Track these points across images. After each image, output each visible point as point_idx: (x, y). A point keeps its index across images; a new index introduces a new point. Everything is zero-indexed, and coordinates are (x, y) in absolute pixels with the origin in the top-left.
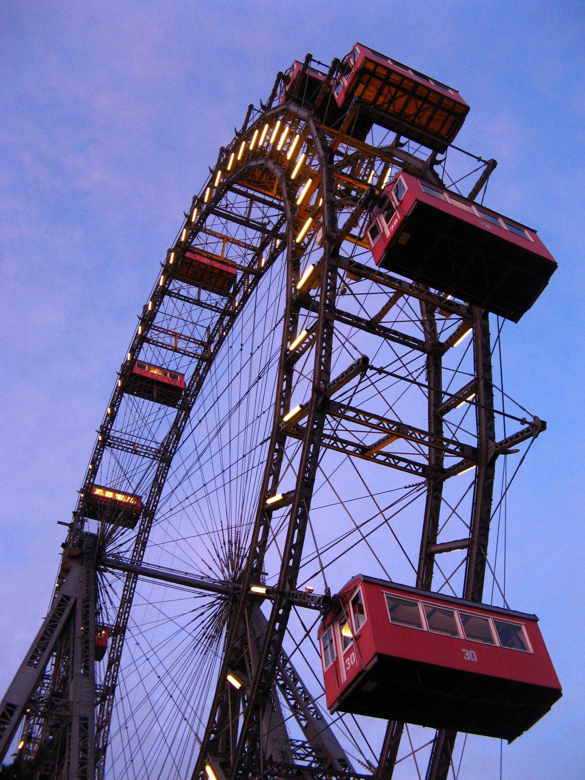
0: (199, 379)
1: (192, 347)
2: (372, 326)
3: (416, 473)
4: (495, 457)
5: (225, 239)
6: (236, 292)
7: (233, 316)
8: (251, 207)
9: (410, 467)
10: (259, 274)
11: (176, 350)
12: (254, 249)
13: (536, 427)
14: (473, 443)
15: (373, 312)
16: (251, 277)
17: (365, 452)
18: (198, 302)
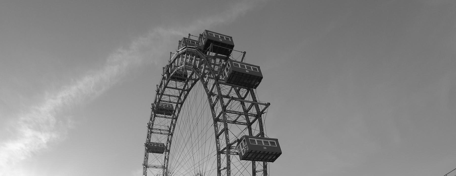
0: (170, 142)
1: (166, 132)
2: (227, 97)
3: (245, 125)
4: (261, 115)
5: (169, 96)
6: (175, 111)
7: (176, 119)
8: (176, 83)
9: (244, 124)
10: (182, 104)
11: (161, 133)
12: (178, 97)
13: (268, 105)
14: (256, 114)
15: (227, 94)
16: (179, 105)
17: (234, 122)
18: (165, 117)
